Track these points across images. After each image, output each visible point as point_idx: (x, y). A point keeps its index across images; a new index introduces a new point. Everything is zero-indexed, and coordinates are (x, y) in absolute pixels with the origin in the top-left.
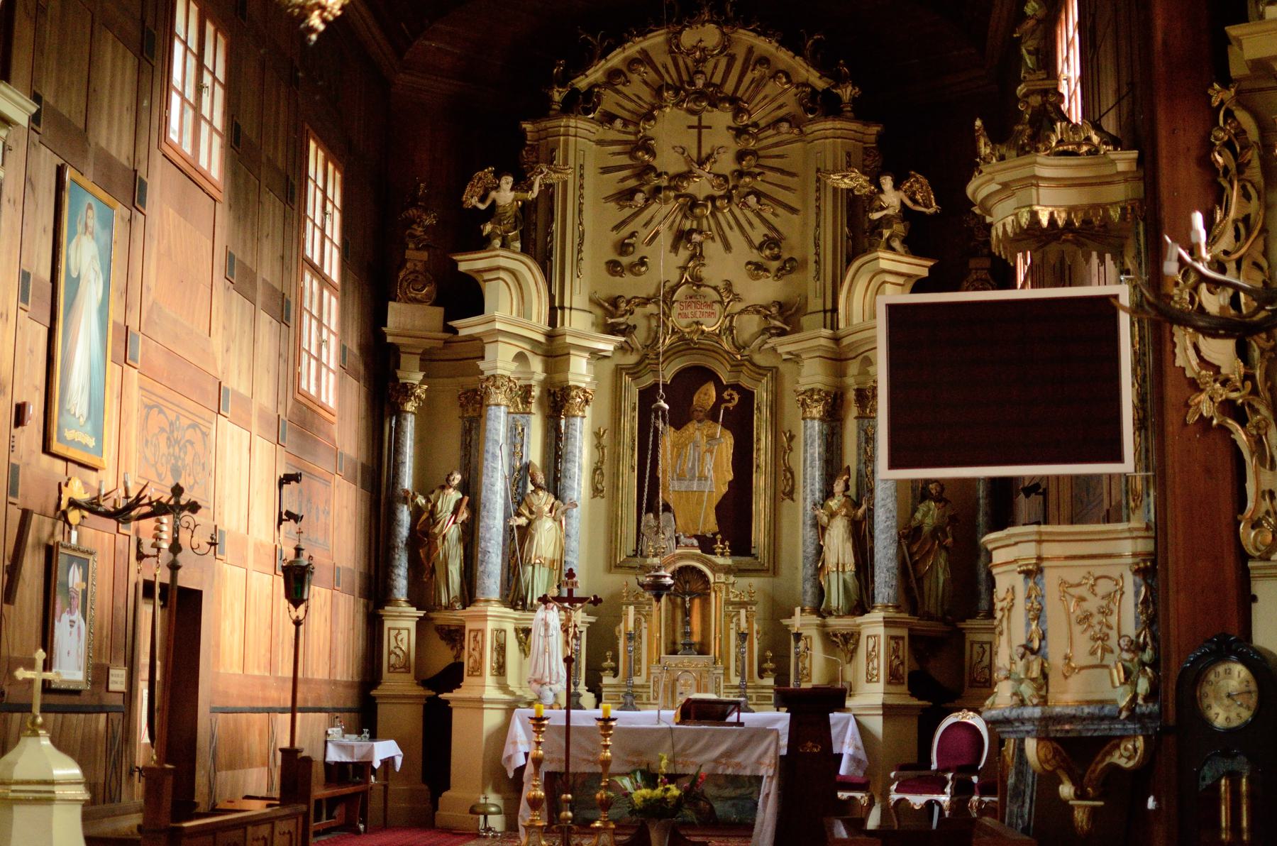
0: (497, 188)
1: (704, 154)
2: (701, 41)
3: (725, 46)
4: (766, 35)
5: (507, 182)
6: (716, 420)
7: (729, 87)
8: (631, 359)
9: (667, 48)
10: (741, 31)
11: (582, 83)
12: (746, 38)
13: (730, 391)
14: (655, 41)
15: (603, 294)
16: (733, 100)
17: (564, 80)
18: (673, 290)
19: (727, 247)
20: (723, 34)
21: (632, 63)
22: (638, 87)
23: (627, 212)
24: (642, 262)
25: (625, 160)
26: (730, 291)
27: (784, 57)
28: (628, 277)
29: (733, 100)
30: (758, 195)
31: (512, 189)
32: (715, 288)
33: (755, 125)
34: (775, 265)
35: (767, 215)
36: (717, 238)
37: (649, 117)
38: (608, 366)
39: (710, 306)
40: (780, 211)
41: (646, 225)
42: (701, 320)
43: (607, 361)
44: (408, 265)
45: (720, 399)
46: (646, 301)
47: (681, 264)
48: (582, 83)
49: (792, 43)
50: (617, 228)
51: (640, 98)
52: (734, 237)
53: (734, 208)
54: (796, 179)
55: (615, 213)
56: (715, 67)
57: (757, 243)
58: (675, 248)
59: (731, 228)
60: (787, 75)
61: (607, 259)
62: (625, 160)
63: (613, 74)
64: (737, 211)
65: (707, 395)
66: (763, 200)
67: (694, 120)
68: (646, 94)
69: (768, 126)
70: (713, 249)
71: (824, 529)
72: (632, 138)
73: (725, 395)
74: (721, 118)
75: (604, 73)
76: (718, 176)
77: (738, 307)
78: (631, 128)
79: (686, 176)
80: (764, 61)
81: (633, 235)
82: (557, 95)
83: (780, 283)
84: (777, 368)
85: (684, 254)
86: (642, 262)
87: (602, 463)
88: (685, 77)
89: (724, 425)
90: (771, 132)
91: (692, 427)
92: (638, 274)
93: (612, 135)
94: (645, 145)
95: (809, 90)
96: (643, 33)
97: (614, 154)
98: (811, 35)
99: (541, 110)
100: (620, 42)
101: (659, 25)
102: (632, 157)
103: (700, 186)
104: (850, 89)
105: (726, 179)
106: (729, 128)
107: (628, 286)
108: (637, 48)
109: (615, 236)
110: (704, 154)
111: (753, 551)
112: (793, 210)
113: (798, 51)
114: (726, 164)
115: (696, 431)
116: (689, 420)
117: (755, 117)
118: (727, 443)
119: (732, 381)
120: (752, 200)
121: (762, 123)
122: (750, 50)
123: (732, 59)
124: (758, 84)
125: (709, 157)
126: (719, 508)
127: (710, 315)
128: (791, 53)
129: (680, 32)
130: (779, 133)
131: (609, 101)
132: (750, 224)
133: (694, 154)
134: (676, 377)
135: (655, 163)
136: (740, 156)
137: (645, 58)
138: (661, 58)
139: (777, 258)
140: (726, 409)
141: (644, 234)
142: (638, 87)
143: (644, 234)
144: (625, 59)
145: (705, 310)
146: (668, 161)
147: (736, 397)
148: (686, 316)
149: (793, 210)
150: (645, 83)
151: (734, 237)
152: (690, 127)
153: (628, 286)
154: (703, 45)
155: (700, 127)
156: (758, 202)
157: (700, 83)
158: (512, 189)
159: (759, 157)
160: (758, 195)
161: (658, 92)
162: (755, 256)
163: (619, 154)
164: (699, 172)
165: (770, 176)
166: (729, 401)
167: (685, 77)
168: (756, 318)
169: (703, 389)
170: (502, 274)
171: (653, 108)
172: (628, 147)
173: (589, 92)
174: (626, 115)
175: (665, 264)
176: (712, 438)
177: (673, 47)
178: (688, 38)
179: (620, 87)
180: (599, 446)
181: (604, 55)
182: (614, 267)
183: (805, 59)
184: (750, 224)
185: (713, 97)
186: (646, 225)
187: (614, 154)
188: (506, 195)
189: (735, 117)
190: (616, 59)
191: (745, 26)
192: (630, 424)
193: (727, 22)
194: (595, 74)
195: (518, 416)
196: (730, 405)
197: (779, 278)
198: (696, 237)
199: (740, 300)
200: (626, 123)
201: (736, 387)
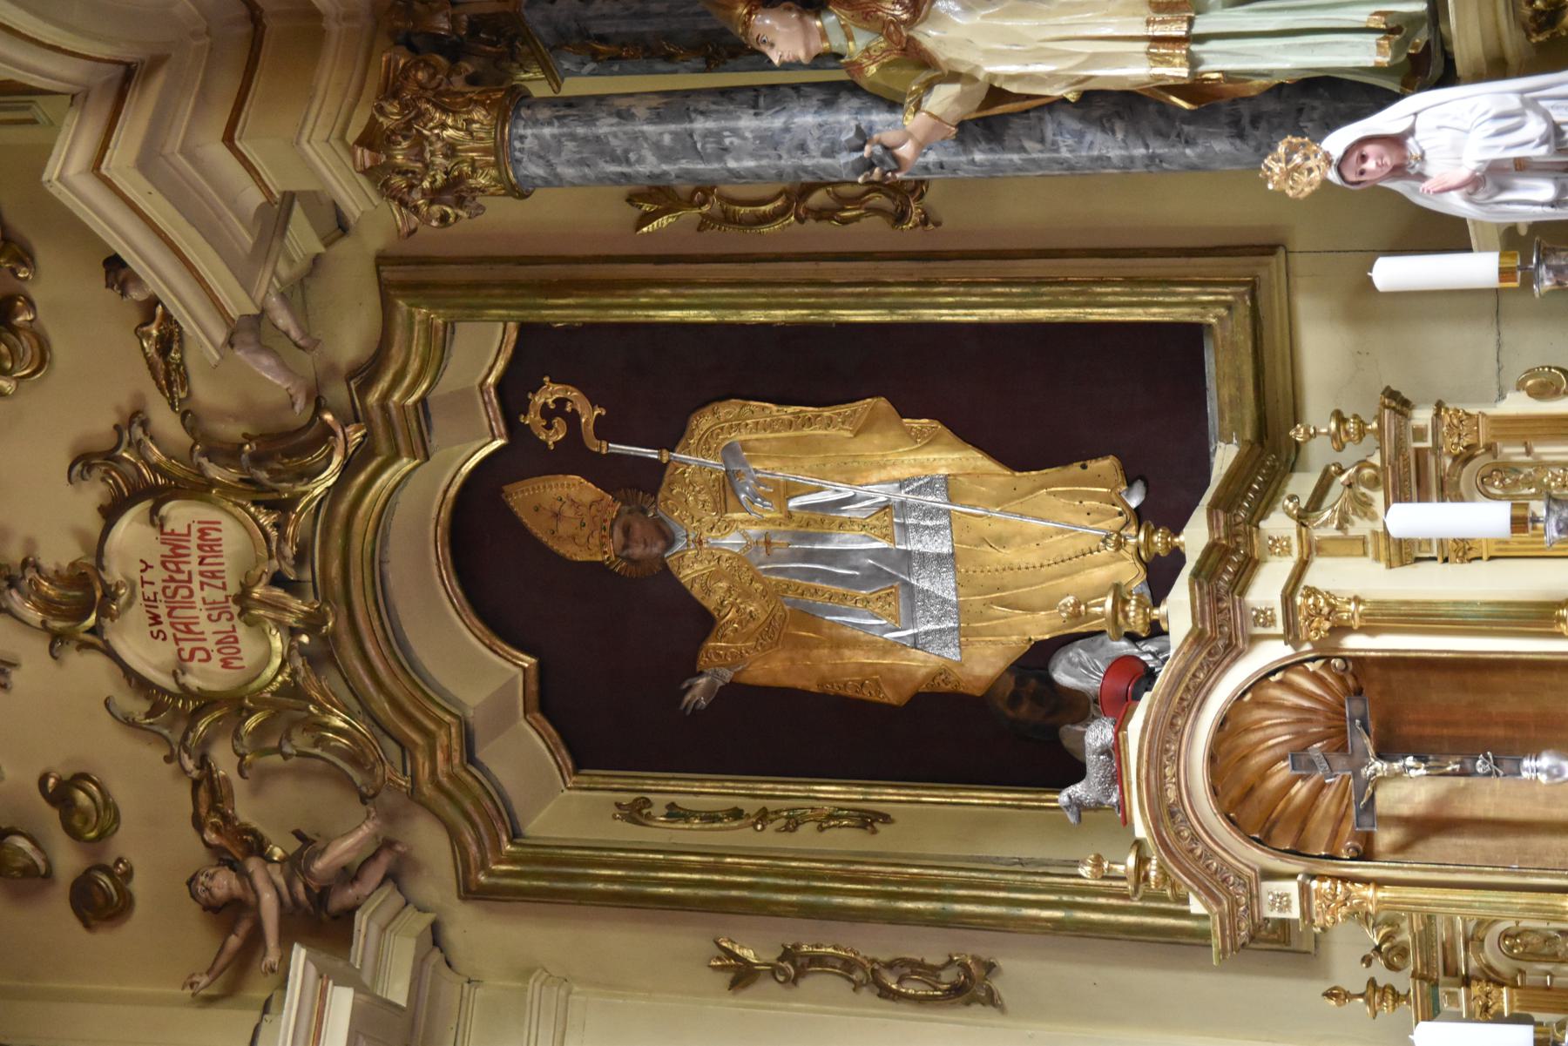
6: (650, 478)
8: (427, 840)
13: (532, 419)
15: (199, 943)
18: (139, 683)
26: (110, 456)
28: (127, 844)
32: (111, 513)
38: (471, 929)
43: (453, 934)
47: (41, 645)
71: (996, 94)
73: (555, 436)
77: (165, 420)
83: (42, 254)
84: (382, 260)
86: (60, 795)
87: (848, 966)
89: (672, 438)
91: (691, 571)
92: (109, 811)
107: (156, 836)
115: (715, 546)
116: (666, 575)
118: (744, 434)
119: (489, 413)
127: (209, 546)
140: (604, 429)
147: (549, 393)
153: (156, 836)
166: (573, 419)
169: (538, 527)
176: (726, 490)
180: (795, 967)
192: (704, 818)
196: (589, 415)
199: (137, 416)
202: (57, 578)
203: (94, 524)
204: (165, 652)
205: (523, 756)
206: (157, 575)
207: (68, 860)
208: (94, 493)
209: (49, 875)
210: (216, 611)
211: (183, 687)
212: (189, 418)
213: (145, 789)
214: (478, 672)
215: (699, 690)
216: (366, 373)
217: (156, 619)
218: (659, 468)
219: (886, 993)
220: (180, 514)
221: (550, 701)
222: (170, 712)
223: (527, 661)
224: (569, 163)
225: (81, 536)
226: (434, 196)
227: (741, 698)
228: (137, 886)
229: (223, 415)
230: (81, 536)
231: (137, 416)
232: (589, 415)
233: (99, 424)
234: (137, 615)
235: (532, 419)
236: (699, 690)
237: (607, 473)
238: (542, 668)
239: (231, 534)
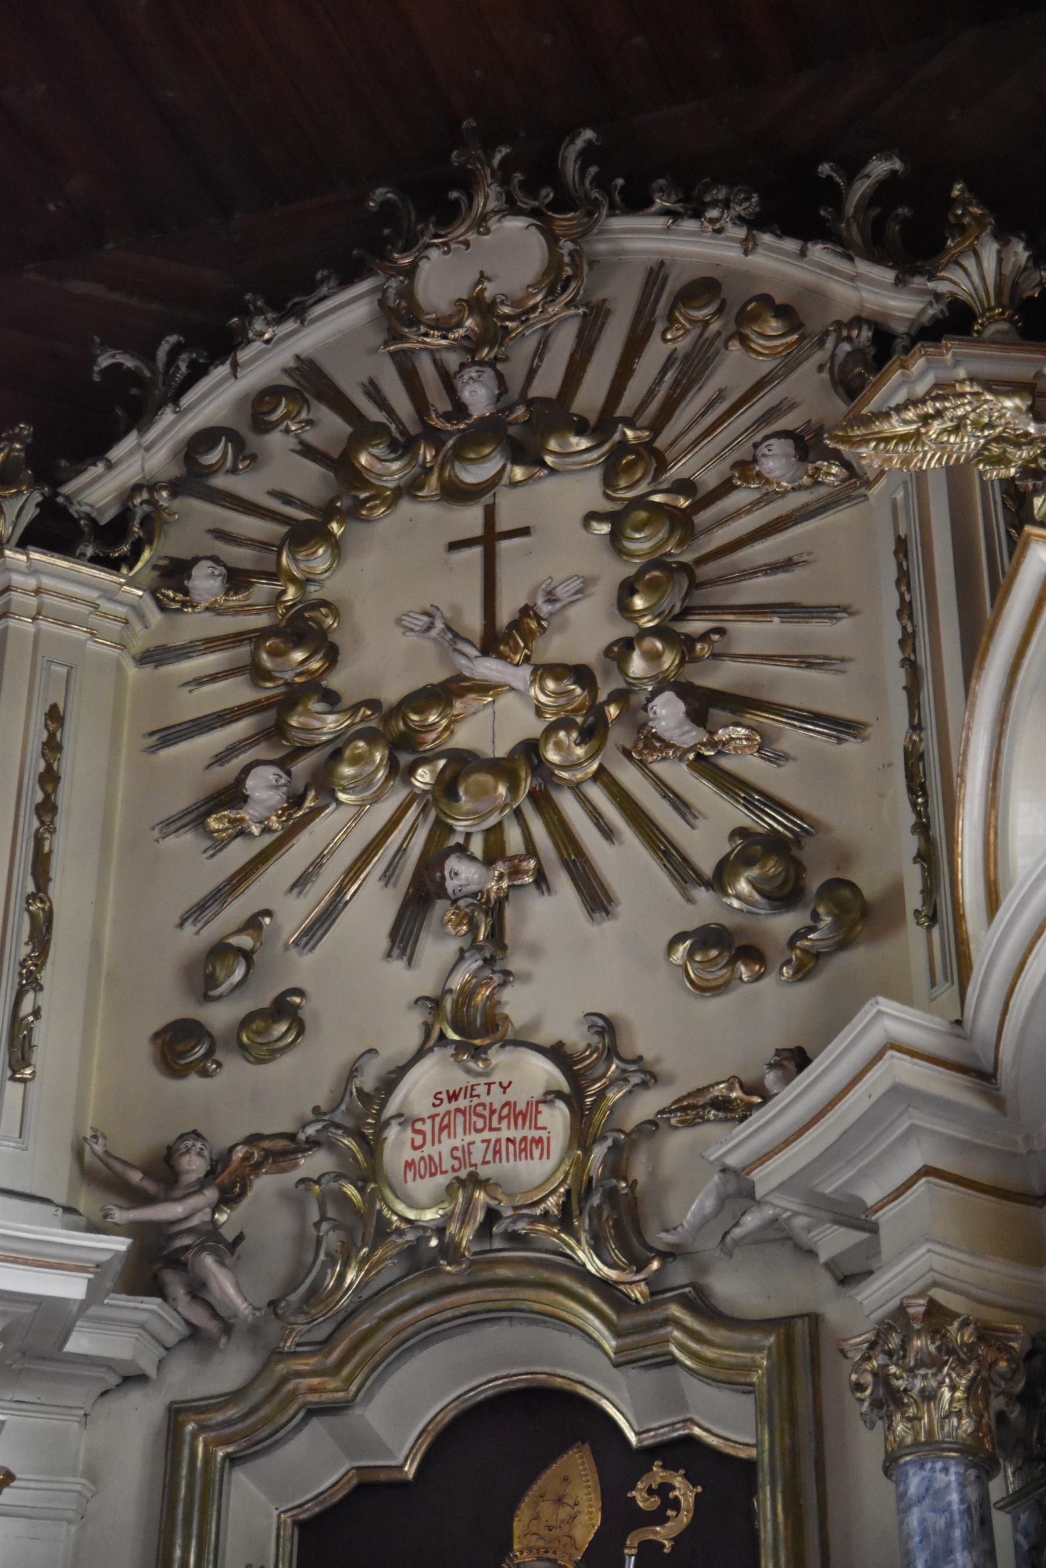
1: (505, 616)
2: (483, 277)
7: (590, 397)
8: (231, 1369)
9: (375, 338)
10: (619, 223)
12: (646, 239)
13: (658, 1474)
14: (339, 323)
15: (134, 1143)
16: (600, 427)
19: (597, 898)
21: (261, 406)
22: (281, 469)
23: (239, 853)
25: (237, 692)
26: (612, 1052)
27: (777, 262)
28: (235, 1072)
30: (702, 705)
32: (557, 1053)
33: (685, 487)
34: (784, 923)
36: (563, 883)
37: (304, 535)
38: (139, 1415)
40: (794, 738)
41: (302, 882)
43: (135, 1396)
45: (620, 1517)
46: (285, 1149)
47: (428, 988)
49: (795, 211)
50: (200, 910)
52: (622, 860)
54: (846, 623)
55: (194, 866)
56: (540, 352)
57: (707, 867)
58: (403, 938)
59: (608, 833)
60: (784, 312)
61: (159, 1022)
62: (237, 692)
63: (205, 439)
64: (629, 777)
66: (717, 714)
67: (469, 519)
68: (308, 480)
69: (727, 487)
70: (549, 914)
74: (561, 500)
75: (175, 454)
77: (647, 1105)
78: (262, 590)
79: (445, 693)
80: (705, 288)
81: (252, 924)
83: (805, 989)
84: (814, 1320)
85: (438, 949)
86: (284, 1008)
93: (195, 625)
94: (306, 627)
95: (866, 334)
96: (290, 301)
97: (199, 682)
98: (853, 168)
100: (220, 345)
101: (349, 275)
102: (258, 674)
105: (582, 674)
106: (592, 517)
107: (239, 1100)
108: (283, 357)
109: (194, 939)
110: (505, 616)
112: (844, 727)
117: (677, 471)
119: (664, 1428)
120: (667, 713)
121: (710, 479)
123: (594, 319)
124: (691, 369)
125: (516, 625)
127: (525, 1148)
128: (791, 245)
130: (767, 498)
131: (191, 522)
132: (681, 805)
133: (473, 622)
134: (450, 1440)
135: (335, 681)
137: (310, 382)
140: (649, 1551)
143: (294, 913)
144: (239, 404)
145: (507, 1132)
146: (384, 660)
147: (684, 1492)
148: (433, 1168)
149: (844, 727)
150: (308, 451)
151: (622, 860)
152: (455, 546)
153: (239, 1100)
154: (490, 290)
155: (489, 539)
157: (478, 396)
159: (695, 585)
162: (705, 908)
163: (214, 678)
164: (489, 669)
165: (748, 633)
166: (658, 1518)
167: (440, 402)
169: (548, 1480)
171: (329, 512)
174: (240, 556)
175: (366, 989)
177: (400, 316)
178: (440, 277)
179: (220, 481)
184: (681, 805)
185: (525, 434)
186: (302, 882)
187: (199, 682)
189: (609, 481)
190: (216, 398)
191: (636, 202)
193: (562, 204)
194: (141, 457)
196: (664, 1534)
197: (803, 972)
199: (651, 1078)
200: (237, 580)
201: (683, 1452)
202: (493, 1002)
203: (546, 1037)
204: (422, 1107)
205: (313, 1467)
206: (497, 1098)
207: (220, 1016)
208: (576, 1037)
209: (207, 999)
210: (461, 1155)
211: (387, 1123)
212: (651, 1128)
213: (288, 1087)
214: (400, 1417)
216: (700, 1302)
217: (453, 1097)
220: (556, 1120)
221: (370, 1496)
222: (362, 1111)
223: (410, 1470)
224: (923, 1521)
225: (534, 1025)
226: (881, 1377)
228: (194, 1081)
229: (655, 1159)
230: (534, 1025)
231: (651, 1078)
232: (664, 1534)
233: (643, 1042)
234: (459, 1079)
235: (658, 1474)
238: (403, 1485)
239: (538, 1170)
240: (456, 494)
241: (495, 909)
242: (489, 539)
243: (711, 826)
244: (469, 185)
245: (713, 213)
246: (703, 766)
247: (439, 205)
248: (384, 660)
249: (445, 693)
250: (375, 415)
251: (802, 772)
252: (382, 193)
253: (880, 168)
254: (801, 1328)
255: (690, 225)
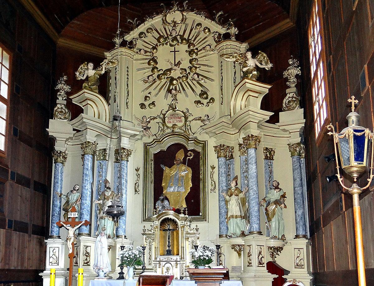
0: (88, 69)
3: (183, 20)
4: (200, 14)
5: (91, 65)
7: (186, 36)
11: (128, 38)
12: (193, 17)
14: (157, 21)
16: (188, 41)
17: (122, 35)
19: (187, 96)
20: (183, 15)
21: (149, 30)
23: (148, 85)
24: (153, 103)
27: (207, 23)
29: (188, 41)
31: (93, 69)
32: (183, 112)
34: (205, 101)
35: (202, 82)
37: (154, 48)
39: (180, 118)
42: (176, 124)
43: (139, 141)
44: (58, 106)
45: (186, 156)
48: (128, 38)
51: (151, 42)
53: (188, 80)
58: (166, 97)
65: (180, 155)
72: (149, 57)
76: (182, 69)
81: (149, 93)
82: (118, 41)
86: (153, 103)
88: (169, 33)
90: (203, 51)
99: (111, 46)
100: (143, 21)
101: (158, 14)
103: (176, 74)
104: (234, 28)
106: (186, 51)
107: (149, 112)
111: (201, 214)
112: (212, 80)
113: (213, 19)
114: (185, 64)
122: (194, 21)
123: (187, 25)
126: (187, 199)
129: (166, 16)
131: (139, 44)
136: (191, 61)
138: (160, 27)
139: (207, 98)
141: (154, 93)
142: (151, 38)
146: (163, 65)
149: (212, 80)
151: (189, 91)
153: (149, 112)
155: (175, 51)
156: (198, 77)
158: (93, 69)
160: (198, 75)
161: (158, 40)
162: (198, 98)
165: (202, 68)
166: (190, 156)
168: (199, 122)
170: (89, 102)
172: (147, 61)
173: (131, 43)
175: (163, 102)
177: (164, 22)
178: (169, 18)
181: (138, 26)
182: (142, 106)
183: (216, 22)
188: (91, 72)
189: (189, 47)
190: (142, 28)
195: (101, 161)
198: (173, 92)
211: (166, 117)
213: (154, 112)
215: (162, 166)
217: (172, 115)
218: (185, 164)
219: (136, 184)
224: (221, 163)
227: (162, 171)
236: (162, 166)
237: (185, 159)
240: (171, 45)
241: (175, 95)
242: (175, 51)
243: (198, 89)
244: (173, 5)
245: (201, 15)
246: (198, 83)
247: (169, 7)
248: (163, 65)
249: (170, 70)
250: (162, 34)
251: (207, 84)
252: (162, 4)
253: (220, 13)
254: (206, 142)
255: (198, 15)
